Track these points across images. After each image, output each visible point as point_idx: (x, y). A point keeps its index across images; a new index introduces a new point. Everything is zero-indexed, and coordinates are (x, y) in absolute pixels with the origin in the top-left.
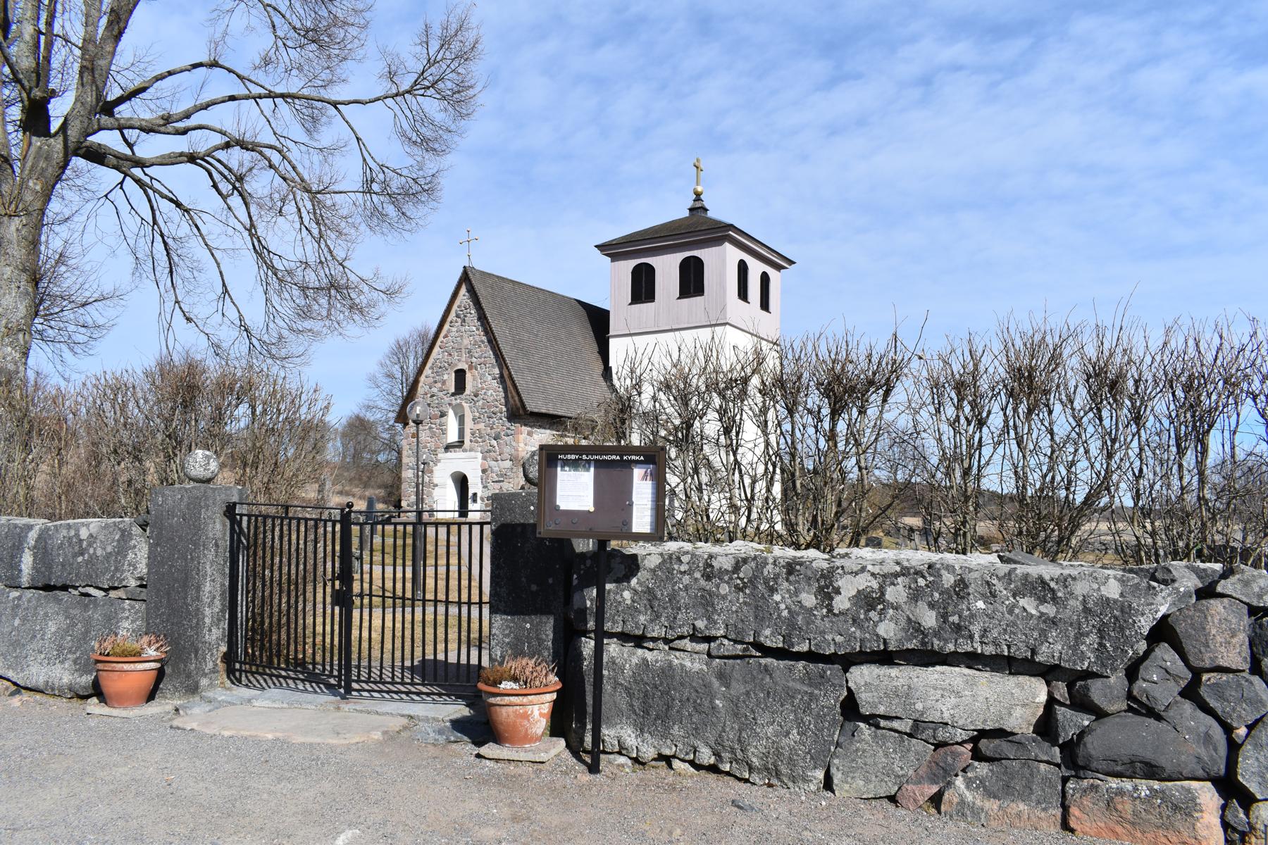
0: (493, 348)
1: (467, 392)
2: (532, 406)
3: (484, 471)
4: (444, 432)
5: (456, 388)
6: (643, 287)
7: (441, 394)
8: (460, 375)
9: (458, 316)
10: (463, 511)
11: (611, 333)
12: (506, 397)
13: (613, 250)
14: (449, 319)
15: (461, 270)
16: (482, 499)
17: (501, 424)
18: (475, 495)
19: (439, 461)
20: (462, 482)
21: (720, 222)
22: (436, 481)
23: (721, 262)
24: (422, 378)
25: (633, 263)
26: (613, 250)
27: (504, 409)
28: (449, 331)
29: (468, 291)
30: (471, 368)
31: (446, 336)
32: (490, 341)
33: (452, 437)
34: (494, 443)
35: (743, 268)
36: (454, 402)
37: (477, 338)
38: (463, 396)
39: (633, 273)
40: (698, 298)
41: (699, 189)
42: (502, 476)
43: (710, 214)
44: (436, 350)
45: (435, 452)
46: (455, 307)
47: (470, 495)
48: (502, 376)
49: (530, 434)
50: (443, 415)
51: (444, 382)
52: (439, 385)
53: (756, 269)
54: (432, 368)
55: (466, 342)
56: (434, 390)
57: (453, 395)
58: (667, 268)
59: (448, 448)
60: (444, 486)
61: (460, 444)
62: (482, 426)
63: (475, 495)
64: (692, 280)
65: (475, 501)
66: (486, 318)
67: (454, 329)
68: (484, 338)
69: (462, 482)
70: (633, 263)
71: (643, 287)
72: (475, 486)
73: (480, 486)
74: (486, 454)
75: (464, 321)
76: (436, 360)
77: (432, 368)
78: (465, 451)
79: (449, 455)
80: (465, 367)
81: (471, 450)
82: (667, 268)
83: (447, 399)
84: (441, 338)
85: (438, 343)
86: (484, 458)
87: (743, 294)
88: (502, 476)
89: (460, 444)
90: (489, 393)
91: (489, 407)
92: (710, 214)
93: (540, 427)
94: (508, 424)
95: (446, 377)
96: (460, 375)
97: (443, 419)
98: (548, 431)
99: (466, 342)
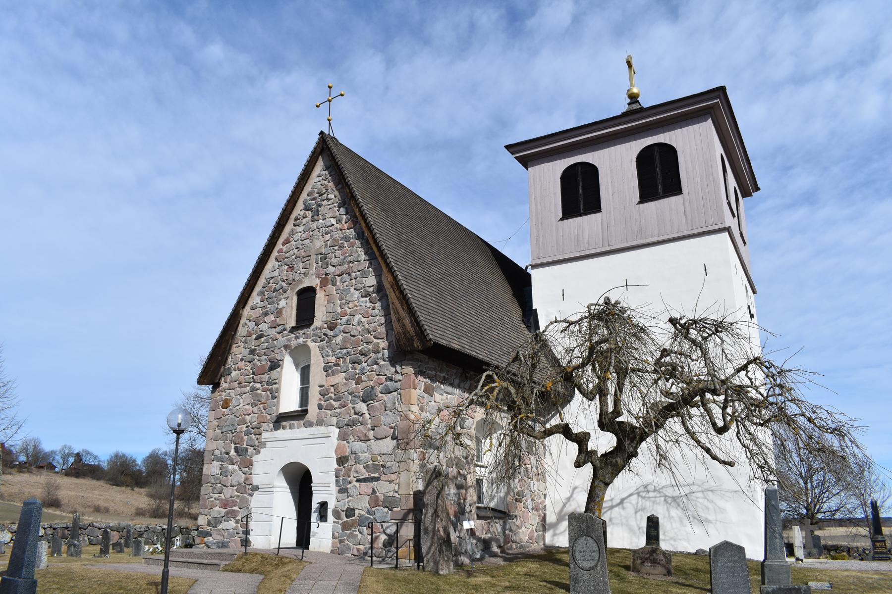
0: (366, 245)
1: (317, 323)
2: (441, 333)
3: (341, 461)
4: (275, 395)
5: (297, 321)
6: (581, 194)
7: (273, 332)
8: (306, 297)
9: (307, 208)
10: (303, 539)
12: (388, 323)
13: (529, 153)
14: (293, 216)
15: (316, 138)
16: (337, 514)
17: (380, 369)
18: (324, 505)
19: (263, 445)
20: (300, 481)
22: (256, 480)
24: (246, 312)
25: (562, 165)
26: (529, 153)
27: (383, 344)
28: (292, 233)
29: (327, 168)
30: (325, 281)
31: (287, 242)
32: (360, 236)
33: (289, 402)
34: (362, 407)
36: (294, 343)
37: (337, 235)
38: (309, 331)
39: (561, 178)
40: (673, 199)
41: (635, 90)
42: (375, 468)
44: (271, 263)
46: (304, 196)
47: (315, 505)
48: (380, 289)
49: (428, 391)
50: (275, 365)
51: (279, 313)
52: (272, 317)
54: (261, 293)
55: (319, 243)
56: (264, 327)
57: (293, 330)
58: (616, 166)
59: (281, 420)
60: (269, 490)
61: (300, 415)
62: (340, 378)
63: (324, 505)
64: (659, 176)
65: (323, 517)
66: (353, 197)
67: (299, 229)
68: (351, 233)
69: (300, 481)
70: (562, 165)
71: (581, 194)
72: (324, 490)
73: (334, 488)
74: (346, 430)
75: (317, 213)
76: (268, 280)
77: (261, 293)
78: (309, 425)
79: (280, 433)
80: (315, 282)
81: (320, 423)
82: (616, 166)
83: (282, 340)
84: (279, 245)
85: (275, 253)
86: (343, 437)
88: (375, 468)
89: (300, 415)
90: (355, 320)
91: (355, 345)
93: (444, 381)
94: (390, 370)
95: (282, 303)
96: (306, 297)
98: (457, 391)
99: (319, 243)
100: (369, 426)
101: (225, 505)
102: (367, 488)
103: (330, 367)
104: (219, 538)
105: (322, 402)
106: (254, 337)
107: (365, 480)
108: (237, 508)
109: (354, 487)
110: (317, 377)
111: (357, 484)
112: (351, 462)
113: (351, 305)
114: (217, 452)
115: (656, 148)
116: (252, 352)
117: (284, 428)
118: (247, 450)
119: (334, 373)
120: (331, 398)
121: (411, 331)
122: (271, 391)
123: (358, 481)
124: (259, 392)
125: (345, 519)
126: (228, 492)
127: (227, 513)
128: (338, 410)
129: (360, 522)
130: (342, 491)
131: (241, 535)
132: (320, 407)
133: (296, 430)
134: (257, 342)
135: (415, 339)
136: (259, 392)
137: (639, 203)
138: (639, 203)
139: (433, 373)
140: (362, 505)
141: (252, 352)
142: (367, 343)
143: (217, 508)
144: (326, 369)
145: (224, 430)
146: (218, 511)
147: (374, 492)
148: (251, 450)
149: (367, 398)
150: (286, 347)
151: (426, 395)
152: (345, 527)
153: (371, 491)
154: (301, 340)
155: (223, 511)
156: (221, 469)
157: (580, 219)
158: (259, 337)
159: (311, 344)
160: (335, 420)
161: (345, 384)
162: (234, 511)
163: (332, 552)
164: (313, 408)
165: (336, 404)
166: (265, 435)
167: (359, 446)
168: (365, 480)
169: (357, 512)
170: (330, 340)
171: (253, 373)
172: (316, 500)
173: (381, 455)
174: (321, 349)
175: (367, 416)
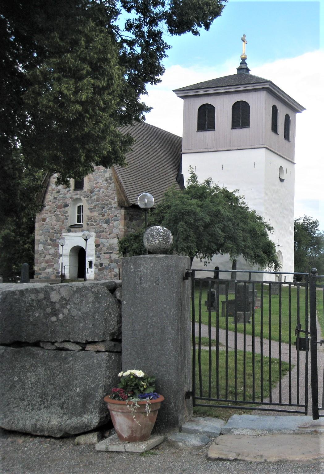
3: (97, 246)
6: (206, 119)
11: (183, 151)
16: (95, 265)
18: (91, 263)
20: (80, 253)
21: (265, 80)
23: (259, 106)
34: (105, 226)
35: (275, 111)
36: (75, 197)
43: (251, 73)
45: (60, 232)
53: (282, 112)
62: (95, 214)
64: (241, 116)
69: (80, 253)
72: (90, 257)
73: (94, 256)
74: (99, 234)
79: (71, 234)
82: (223, 108)
86: (98, 237)
87: (274, 128)
92: (251, 73)
97: (66, 209)
100: (108, 233)
101: (47, 262)
102: (107, 256)
103: (92, 209)
104: (45, 275)
105: (89, 223)
106: (56, 191)
107: (107, 253)
108: (53, 263)
109: (103, 256)
110: (86, 213)
111: (104, 255)
112: (101, 246)
113: (99, 184)
114: (41, 240)
115: (241, 103)
116: (55, 198)
117: (72, 232)
118: (56, 240)
119: (94, 211)
120: (92, 221)
121: (124, 199)
122: (66, 216)
123: (104, 253)
124: (60, 216)
125: (100, 267)
126: (48, 257)
127: (48, 265)
128: (95, 226)
129: (106, 268)
130: (98, 257)
131: (55, 274)
132: (88, 224)
133: (77, 233)
134: (57, 194)
135: (125, 202)
136: (60, 216)
137: (232, 129)
138: (232, 129)
139: (132, 213)
140: (105, 262)
141: (55, 198)
142: (107, 201)
143: (43, 264)
144: (90, 209)
145: (44, 231)
146: (43, 265)
147: (110, 257)
148: (57, 240)
149: (107, 222)
150: (71, 198)
151: (130, 222)
152: (100, 270)
153: (109, 257)
154: (78, 196)
155: (46, 265)
156: (43, 247)
157: (205, 132)
158: (59, 192)
159: (82, 198)
160: (93, 230)
161: (98, 216)
162: (52, 264)
163: (95, 279)
164: (84, 223)
165: (94, 224)
166: (63, 234)
167: (104, 240)
168: (107, 253)
169: (104, 265)
170: (91, 197)
171: (56, 207)
172: (88, 259)
173: (113, 244)
174: (87, 201)
175: (107, 229)
